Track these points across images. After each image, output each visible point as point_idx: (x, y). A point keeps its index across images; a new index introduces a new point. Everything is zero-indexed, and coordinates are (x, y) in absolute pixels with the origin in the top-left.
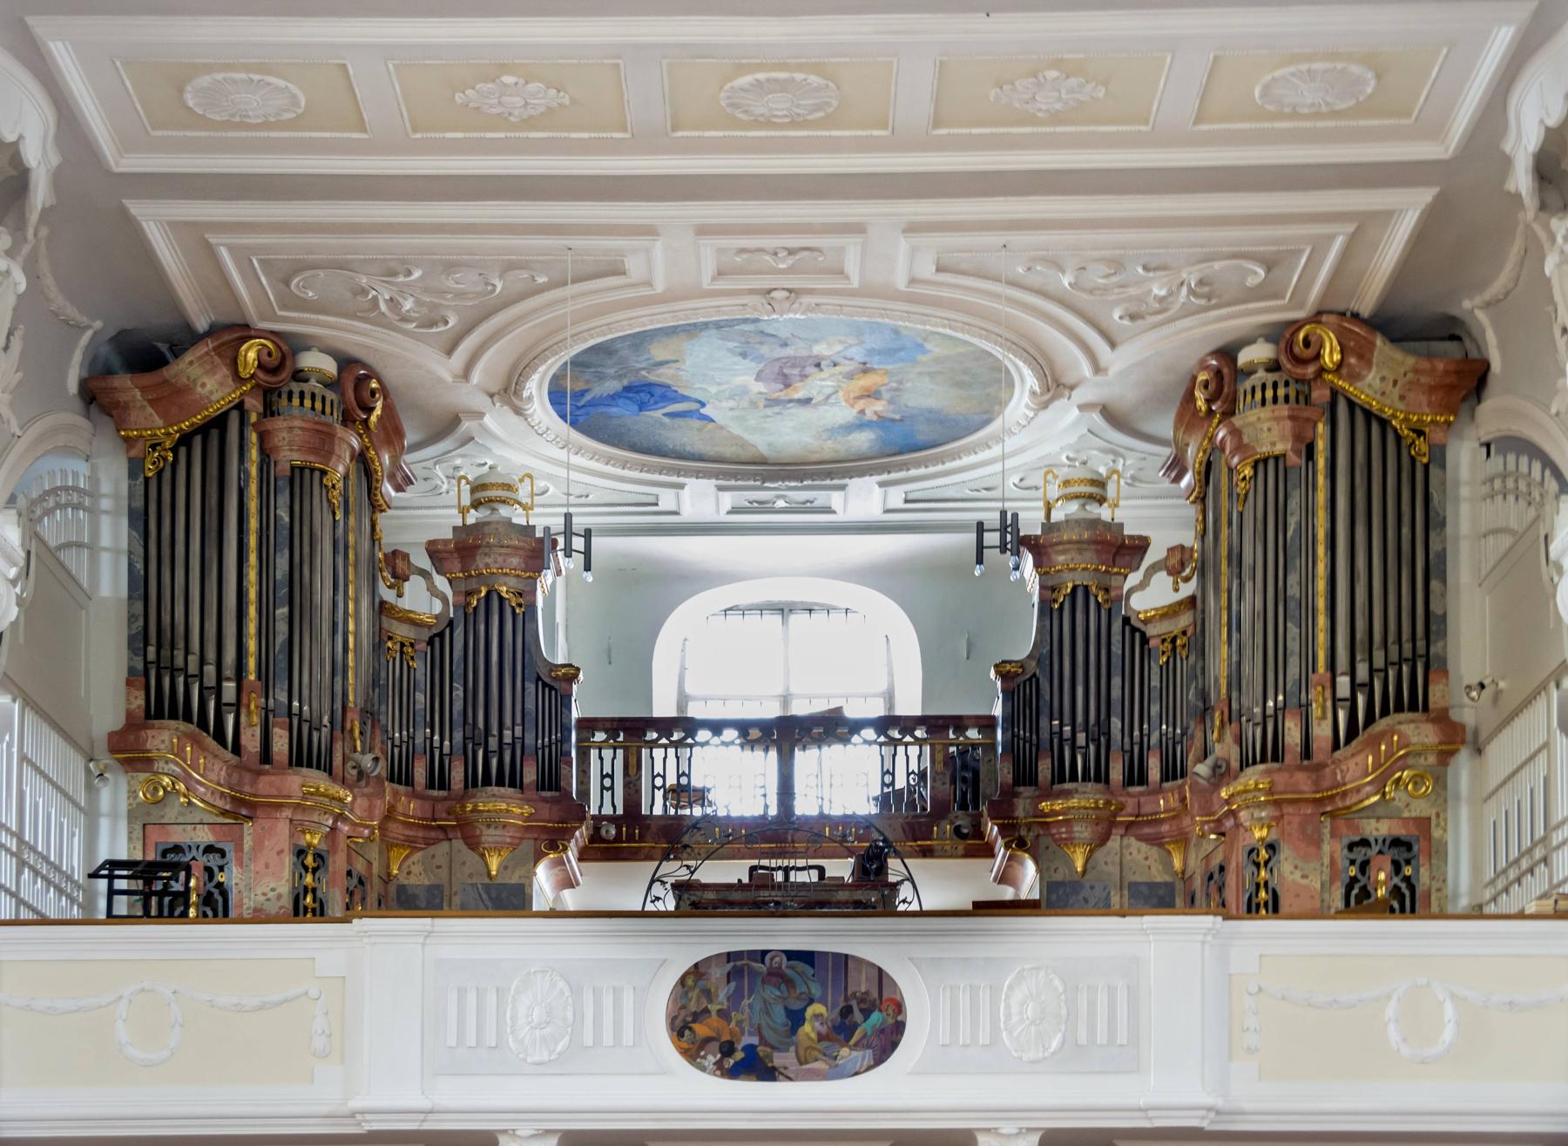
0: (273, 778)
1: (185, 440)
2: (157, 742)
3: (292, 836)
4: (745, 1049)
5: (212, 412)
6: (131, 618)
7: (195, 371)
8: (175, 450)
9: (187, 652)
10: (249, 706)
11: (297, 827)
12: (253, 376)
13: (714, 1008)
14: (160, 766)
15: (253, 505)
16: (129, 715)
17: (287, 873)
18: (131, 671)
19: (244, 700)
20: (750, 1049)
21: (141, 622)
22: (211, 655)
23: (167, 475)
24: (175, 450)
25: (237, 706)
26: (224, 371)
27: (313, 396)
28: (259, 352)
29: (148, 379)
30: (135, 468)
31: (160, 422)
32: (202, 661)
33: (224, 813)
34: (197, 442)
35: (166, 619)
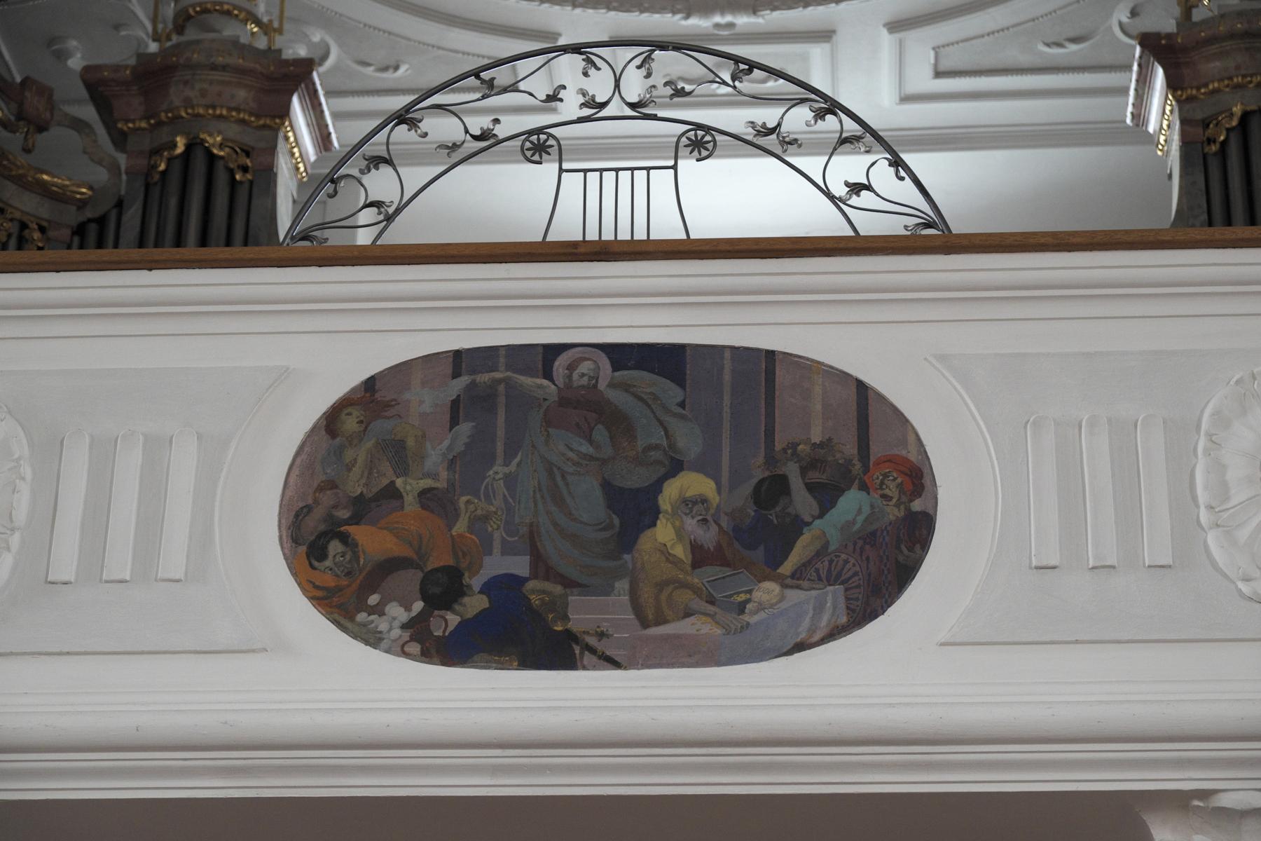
4: (486, 589)
13: (410, 486)
20: (503, 587)
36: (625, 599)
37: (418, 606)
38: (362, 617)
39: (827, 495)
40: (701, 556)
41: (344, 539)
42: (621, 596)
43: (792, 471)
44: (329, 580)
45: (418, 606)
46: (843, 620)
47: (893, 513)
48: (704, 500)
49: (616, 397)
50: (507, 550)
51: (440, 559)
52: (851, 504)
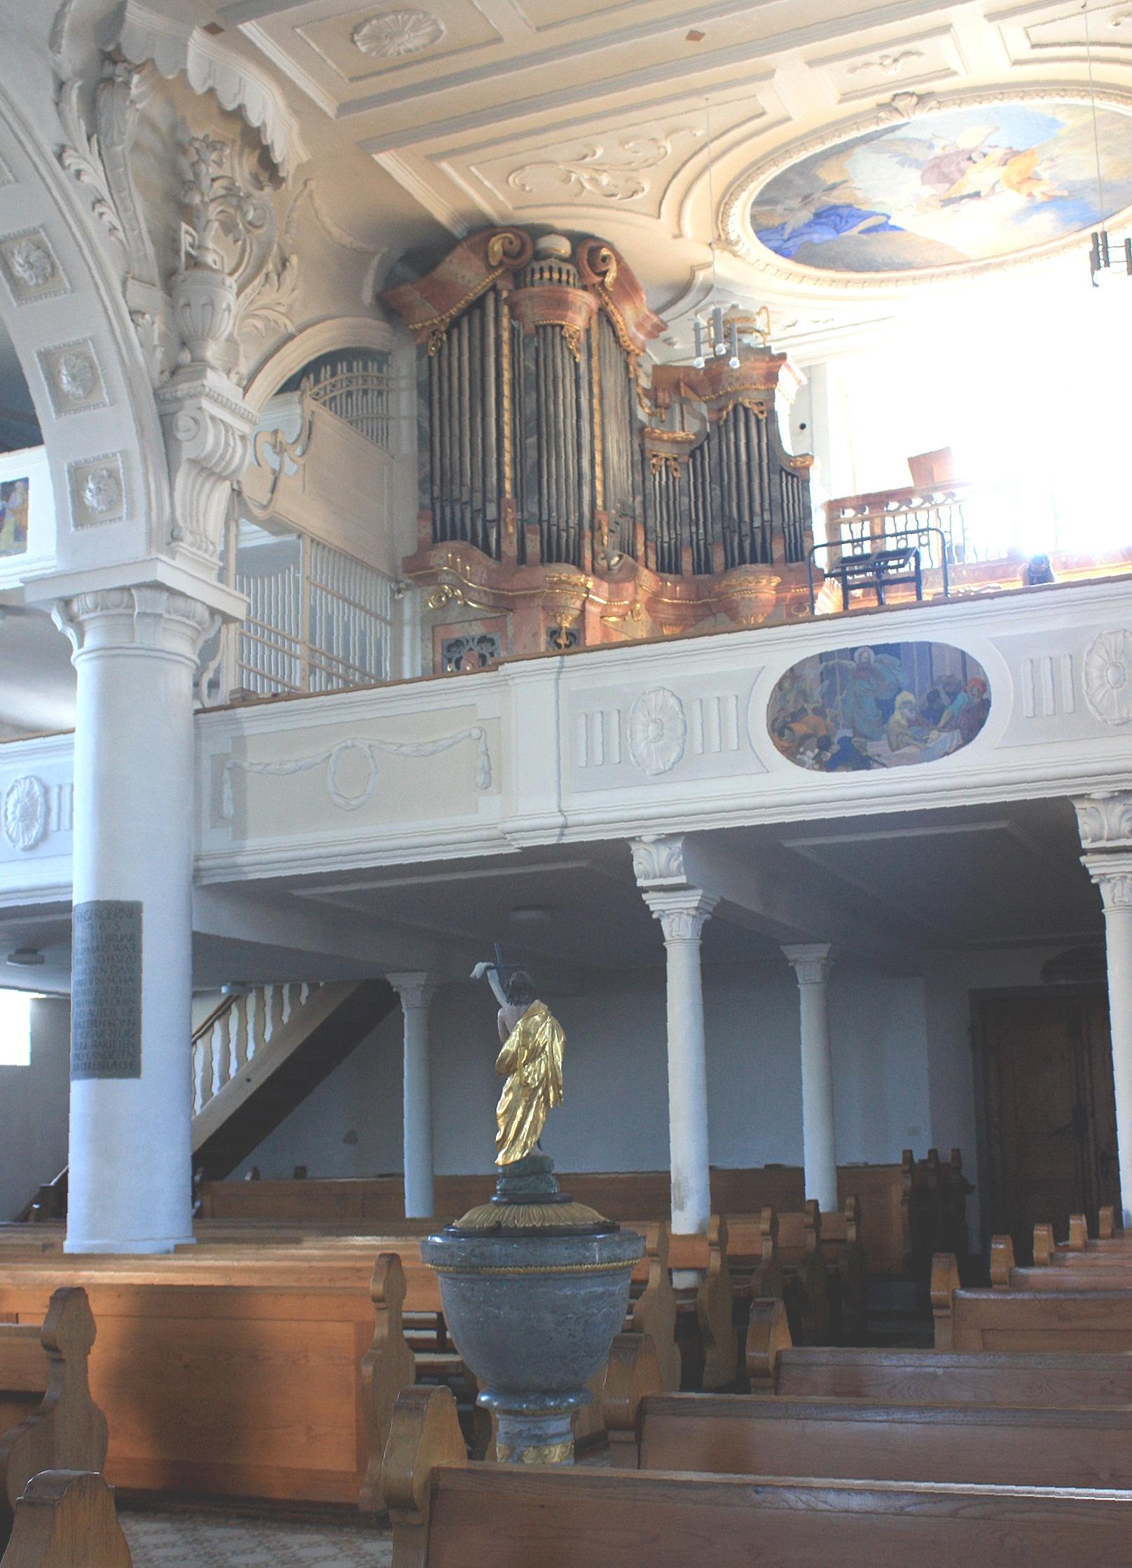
4: (840, 741)
18: (422, 507)
20: (845, 741)
36: (886, 741)
37: (817, 751)
38: (799, 756)
39: (952, 696)
40: (911, 723)
41: (790, 729)
42: (884, 742)
43: (940, 688)
44: (785, 744)
45: (817, 751)
46: (961, 742)
47: (976, 700)
48: (910, 702)
49: (879, 666)
50: (845, 727)
51: (822, 733)
52: (962, 698)
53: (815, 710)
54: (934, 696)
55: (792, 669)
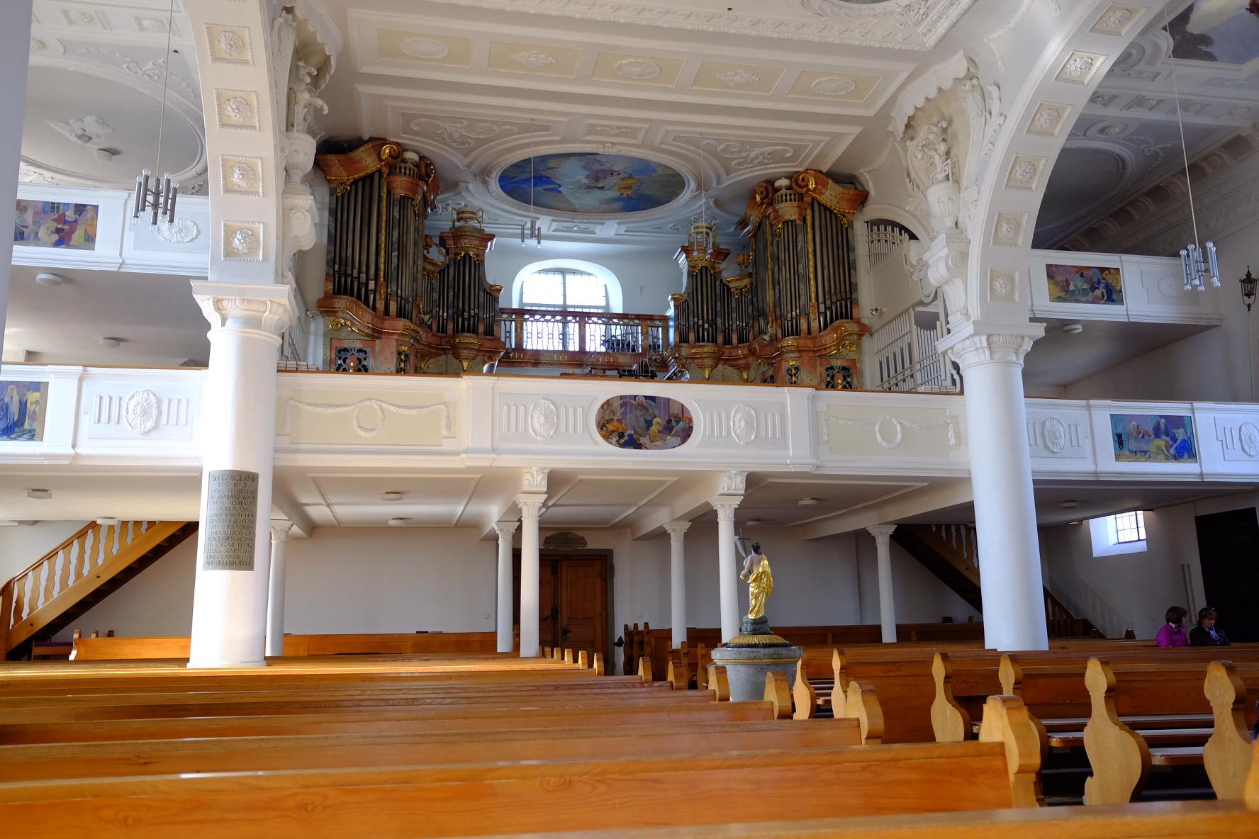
0: (391, 322)
1: (355, 182)
2: (339, 304)
3: (397, 347)
5: (369, 171)
6: (328, 253)
7: (363, 155)
8: (351, 186)
9: (353, 267)
10: (380, 292)
11: (400, 344)
12: (386, 159)
14: (340, 314)
15: (384, 210)
16: (326, 293)
17: (395, 363)
18: (327, 274)
19: (379, 289)
20: (630, 436)
21: (333, 254)
22: (364, 270)
23: (346, 196)
24: (351, 186)
25: (375, 291)
26: (375, 156)
27: (410, 169)
28: (390, 150)
29: (341, 157)
30: (332, 192)
31: (345, 174)
32: (360, 272)
33: (368, 335)
34: (360, 183)
35: (344, 254)
39: (678, 422)
40: (659, 432)
43: (672, 418)
47: (687, 426)
49: (646, 405)
51: (620, 431)
53: (618, 420)
54: (669, 421)
55: (608, 401)
